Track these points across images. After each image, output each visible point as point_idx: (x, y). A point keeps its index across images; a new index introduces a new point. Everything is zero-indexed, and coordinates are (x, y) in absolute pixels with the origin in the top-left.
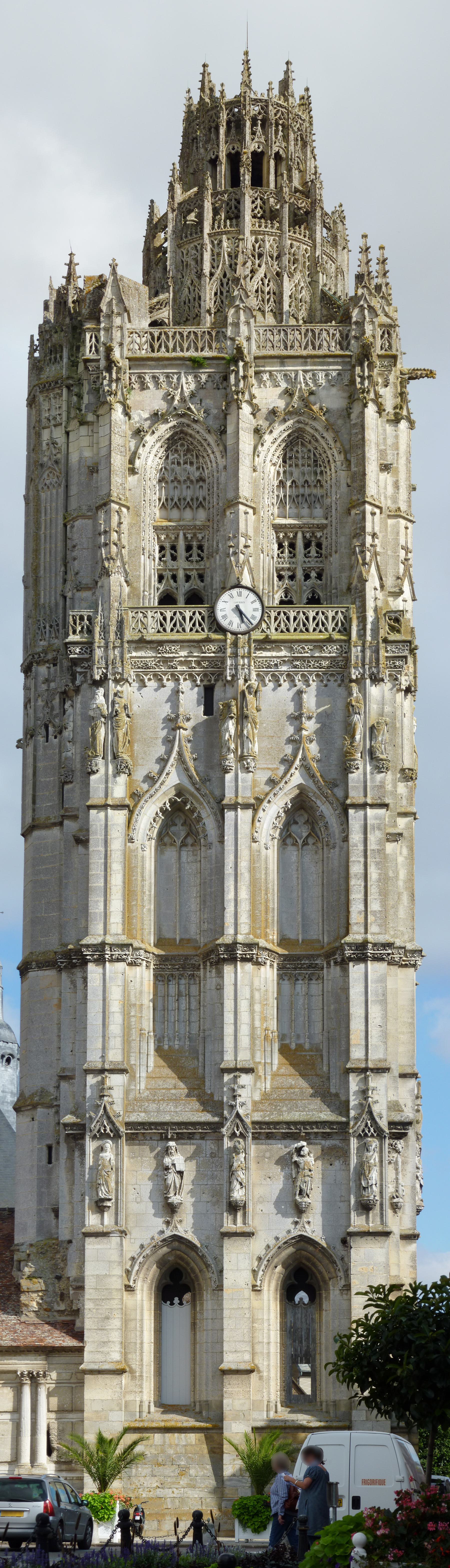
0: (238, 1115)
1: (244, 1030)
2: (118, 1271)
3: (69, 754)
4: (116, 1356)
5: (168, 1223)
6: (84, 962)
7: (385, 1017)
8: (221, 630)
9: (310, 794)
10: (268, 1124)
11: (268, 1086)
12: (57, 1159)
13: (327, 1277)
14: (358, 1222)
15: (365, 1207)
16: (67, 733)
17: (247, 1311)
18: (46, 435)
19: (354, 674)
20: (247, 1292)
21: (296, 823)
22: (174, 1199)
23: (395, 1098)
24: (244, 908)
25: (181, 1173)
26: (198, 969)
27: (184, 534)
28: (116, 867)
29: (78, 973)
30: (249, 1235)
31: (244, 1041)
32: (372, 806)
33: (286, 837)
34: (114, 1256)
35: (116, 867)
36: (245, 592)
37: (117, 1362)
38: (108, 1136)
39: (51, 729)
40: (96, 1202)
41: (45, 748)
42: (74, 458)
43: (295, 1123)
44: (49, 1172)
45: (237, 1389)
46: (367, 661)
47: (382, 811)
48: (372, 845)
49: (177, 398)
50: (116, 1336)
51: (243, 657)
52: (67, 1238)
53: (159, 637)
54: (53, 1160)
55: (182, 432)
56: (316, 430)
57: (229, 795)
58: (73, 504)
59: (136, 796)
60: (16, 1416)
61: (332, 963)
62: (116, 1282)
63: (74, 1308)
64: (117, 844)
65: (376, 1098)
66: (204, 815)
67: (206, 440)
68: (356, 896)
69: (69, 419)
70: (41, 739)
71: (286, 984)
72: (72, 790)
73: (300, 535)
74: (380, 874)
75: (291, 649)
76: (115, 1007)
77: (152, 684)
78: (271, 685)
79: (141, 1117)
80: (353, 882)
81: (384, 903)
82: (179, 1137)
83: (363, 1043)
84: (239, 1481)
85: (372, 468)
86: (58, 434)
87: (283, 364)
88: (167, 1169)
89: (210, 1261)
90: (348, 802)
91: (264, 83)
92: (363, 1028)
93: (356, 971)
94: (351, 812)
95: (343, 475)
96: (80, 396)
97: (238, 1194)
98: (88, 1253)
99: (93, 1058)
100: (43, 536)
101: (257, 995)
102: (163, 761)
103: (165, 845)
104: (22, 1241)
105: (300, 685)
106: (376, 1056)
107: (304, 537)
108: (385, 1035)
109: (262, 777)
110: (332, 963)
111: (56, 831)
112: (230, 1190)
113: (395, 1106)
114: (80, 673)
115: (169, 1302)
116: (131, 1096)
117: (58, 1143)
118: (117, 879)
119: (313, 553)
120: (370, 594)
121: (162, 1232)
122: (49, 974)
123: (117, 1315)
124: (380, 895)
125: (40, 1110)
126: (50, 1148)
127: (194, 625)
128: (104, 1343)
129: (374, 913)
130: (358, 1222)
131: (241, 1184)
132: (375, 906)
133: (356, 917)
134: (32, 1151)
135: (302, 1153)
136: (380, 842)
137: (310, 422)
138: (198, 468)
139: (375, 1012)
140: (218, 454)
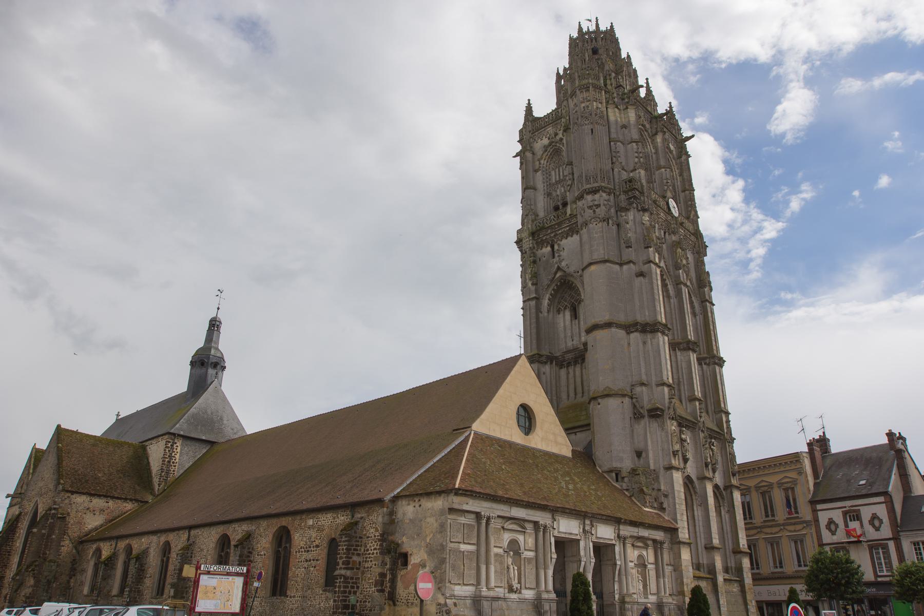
6: (658, 331)
29: (649, 336)
42: (612, 118)
44: (633, 431)
69: (607, 102)
86: (600, 106)
111: (617, 267)
122: (621, 333)
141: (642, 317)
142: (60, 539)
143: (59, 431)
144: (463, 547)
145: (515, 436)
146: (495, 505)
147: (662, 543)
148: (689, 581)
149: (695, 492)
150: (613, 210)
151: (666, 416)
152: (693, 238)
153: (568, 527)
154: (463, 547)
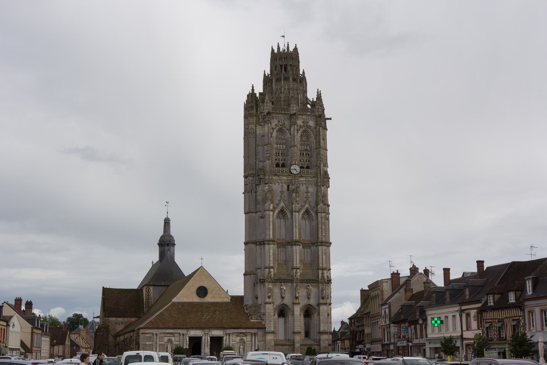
1: (298, 260)
2: (273, 311)
6: (264, 244)
14: (321, 301)
15: (323, 298)
16: (258, 193)
18: (250, 126)
19: (319, 184)
22: (283, 295)
24: (297, 233)
28: (271, 224)
29: (262, 247)
30: (299, 304)
31: (298, 262)
33: (303, 218)
35: (271, 224)
42: (258, 132)
50: (272, 325)
53: (279, 174)
57: (294, 209)
58: (258, 143)
59: (273, 208)
62: (273, 314)
64: (271, 219)
68: (320, 232)
71: (303, 249)
76: (271, 254)
77: (277, 184)
78: (301, 185)
79: (277, 278)
82: (284, 282)
85: (321, 140)
86: (253, 126)
91: (291, 49)
93: (320, 248)
95: (314, 141)
96: (259, 119)
97: (297, 295)
99: (267, 265)
102: (280, 201)
106: (324, 266)
108: (326, 262)
109: (300, 205)
111: (254, 214)
113: (328, 277)
117: (257, 283)
118: (271, 227)
120: (322, 167)
122: (253, 246)
130: (321, 301)
132: (324, 234)
133: (320, 236)
136: (325, 221)
139: (324, 257)
141: (260, 238)
142: (108, 336)
143: (104, 289)
144: (147, 343)
146: (159, 330)
147: (255, 334)
148: (271, 347)
150: (254, 185)
152: (314, 179)
153: (194, 333)
154: (147, 343)
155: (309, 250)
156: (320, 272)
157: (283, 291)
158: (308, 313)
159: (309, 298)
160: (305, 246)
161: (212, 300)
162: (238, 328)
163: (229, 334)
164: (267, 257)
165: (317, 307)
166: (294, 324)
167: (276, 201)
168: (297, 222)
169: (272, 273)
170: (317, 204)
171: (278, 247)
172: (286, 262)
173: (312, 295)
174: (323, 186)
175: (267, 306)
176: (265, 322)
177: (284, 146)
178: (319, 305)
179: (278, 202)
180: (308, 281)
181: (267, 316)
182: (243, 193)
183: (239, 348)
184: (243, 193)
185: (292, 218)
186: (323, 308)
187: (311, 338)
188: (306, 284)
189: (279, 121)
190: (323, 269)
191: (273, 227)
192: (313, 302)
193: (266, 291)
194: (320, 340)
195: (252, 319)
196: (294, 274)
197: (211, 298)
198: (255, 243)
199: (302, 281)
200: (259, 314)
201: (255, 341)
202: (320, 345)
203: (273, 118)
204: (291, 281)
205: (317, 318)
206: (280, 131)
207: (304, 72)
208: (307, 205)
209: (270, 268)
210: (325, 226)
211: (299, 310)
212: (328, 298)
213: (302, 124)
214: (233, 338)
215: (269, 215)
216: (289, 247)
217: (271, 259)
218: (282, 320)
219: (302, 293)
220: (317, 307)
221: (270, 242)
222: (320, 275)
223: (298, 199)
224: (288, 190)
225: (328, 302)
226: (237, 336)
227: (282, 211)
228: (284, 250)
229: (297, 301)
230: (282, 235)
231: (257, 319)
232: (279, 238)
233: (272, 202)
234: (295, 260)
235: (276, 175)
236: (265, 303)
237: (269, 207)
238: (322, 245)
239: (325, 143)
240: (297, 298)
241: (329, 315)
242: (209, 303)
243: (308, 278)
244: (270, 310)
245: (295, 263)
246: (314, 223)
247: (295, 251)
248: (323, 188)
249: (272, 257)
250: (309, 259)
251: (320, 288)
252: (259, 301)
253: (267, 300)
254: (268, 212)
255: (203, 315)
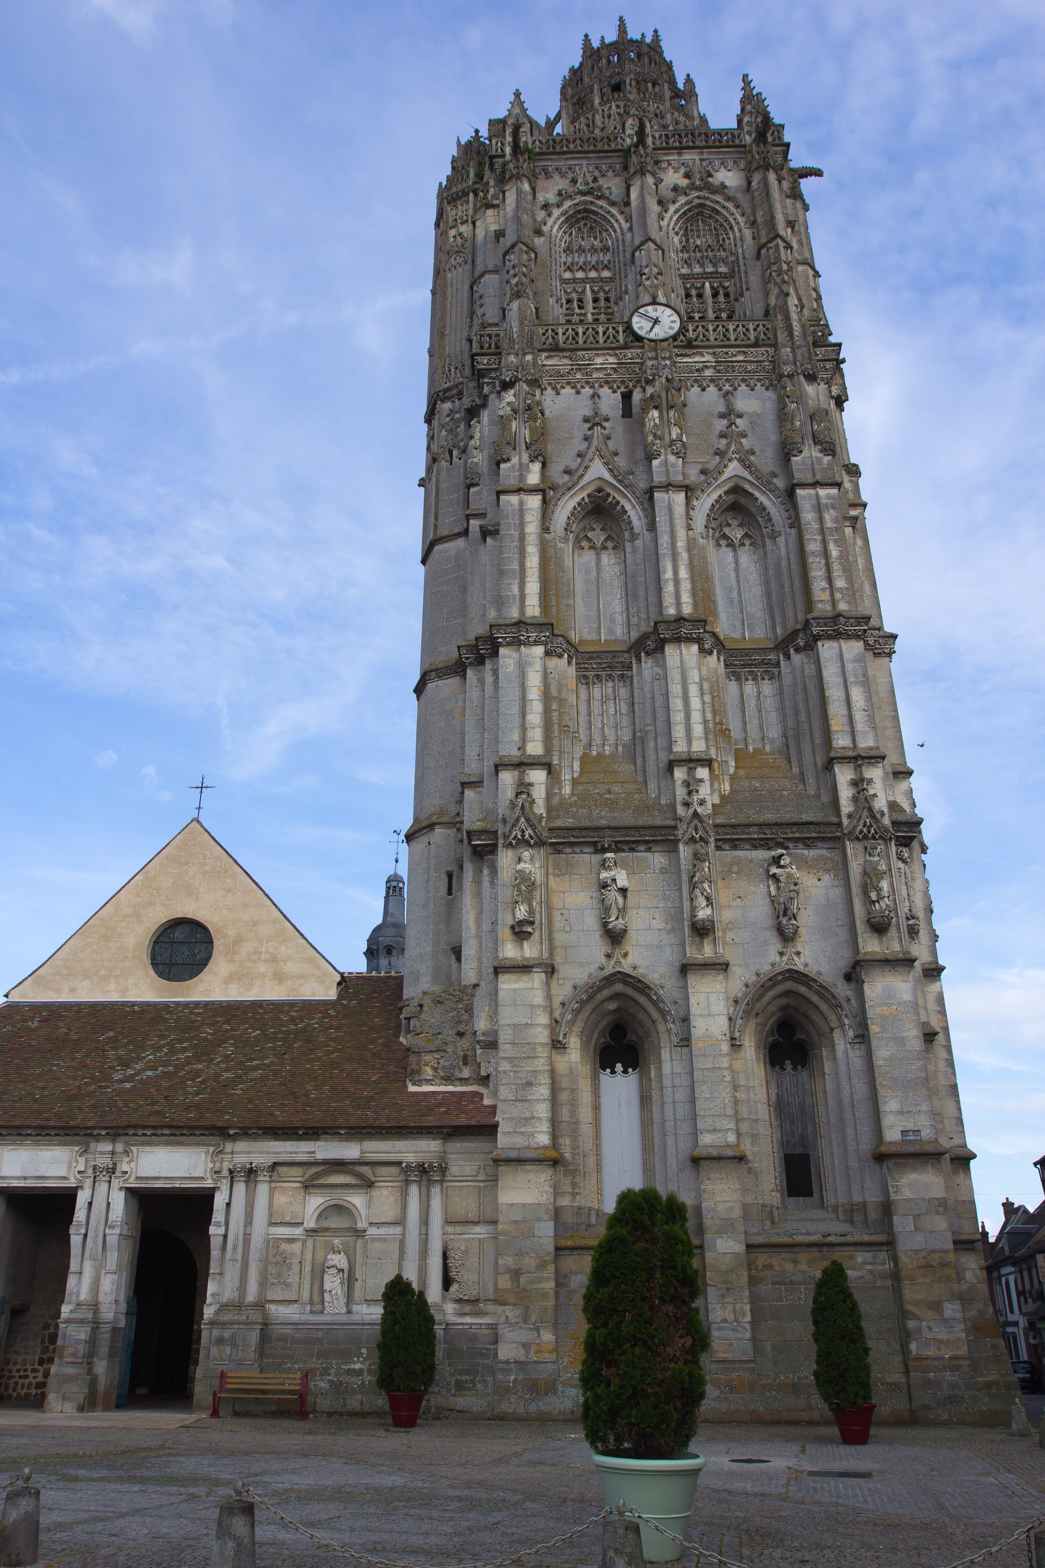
0: (696, 814)
1: (696, 717)
2: (543, 1019)
3: (475, 460)
4: (543, 1139)
5: (608, 956)
7: (869, 699)
8: (639, 339)
9: (747, 487)
10: (733, 826)
11: (727, 788)
12: (460, 888)
13: (826, 1030)
14: (871, 945)
15: (879, 928)
17: (726, 1073)
19: (787, 369)
20: (725, 1047)
21: (729, 525)
22: (616, 923)
23: (890, 798)
24: (686, 586)
25: (623, 891)
26: (630, 668)
27: (591, 288)
31: (698, 730)
32: (823, 485)
34: (539, 998)
36: (660, 308)
37: (545, 1148)
38: (527, 844)
39: (455, 453)
40: (512, 927)
41: (448, 470)
43: (769, 825)
45: (719, 1187)
46: (799, 357)
47: (834, 491)
48: (829, 524)
49: (580, 181)
50: (543, 1110)
51: (664, 359)
52: (473, 980)
54: (454, 892)
55: (586, 210)
56: (717, 202)
57: (658, 478)
60: (398, 1230)
61: (792, 651)
62: (542, 1036)
63: (483, 1073)
65: (872, 792)
66: (628, 507)
67: (609, 212)
68: (817, 573)
70: (444, 464)
71: (733, 686)
72: (480, 492)
73: (707, 285)
74: (840, 551)
75: (714, 354)
76: (534, 694)
80: (810, 560)
81: (850, 579)
83: (847, 729)
84: (733, 1330)
87: (680, 154)
88: (604, 886)
89: (669, 1006)
90: (795, 481)
92: (845, 712)
93: (827, 649)
94: (799, 492)
95: (747, 233)
97: (704, 913)
98: (501, 993)
100: (449, 305)
101: (706, 685)
103: (583, 548)
104: (412, 994)
105: (727, 387)
106: (866, 742)
107: (712, 287)
108: (872, 720)
110: (792, 651)
111: (460, 542)
112: (693, 909)
113: (893, 806)
114: (488, 384)
115: (608, 1071)
116: (555, 801)
117: (461, 868)
119: (721, 298)
121: (602, 969)
122: (450, 684)
123: (545, 1079)
124: (844, 572)
125: (438, 831)
126: (450, 876)
127: (608, 338)
128: (526, 1119)
129: (841, 590)
130: (871, 945)
131: (707, 899)
132: (840, 583)
134: (427, 881)
135: (782, 863)
136: (836, 520)
137: (711, 196)
138: (602, 241)
139: (857, 695)
140: (622, 221)
145: (144, 988)
148: (530, 1262)
149: (663, 1013)
151: (501, 841)
152: (761, 353)
155: (768, 688)
156: (844, 775)
157: (613, 896)
158: (791, 1030)
159: (786, 936)
160: (742, 662)
161: (234, 994)
162: (313, 1133)
163: (251, 1173)
164: (510, 708)
165: (843, 990)
166: (693, 1100)
167: (564, 458)
168: (681, 533)
169: (539, 793)
170: (786, 451)
171: (584, 679)
172: (635, 748)
173: (807, 919)
174: (811, 378)
175: (508, 984)
176: (495, 1094)
177: (606, 274)
178: (853, 975)
179: (573, 464)
180: (776, 836)
181: (505, 1049)
182: (422, 483)
183: (319, 1272)
184: (422, 483)
185: (652, 526)
186: (886, 991)
187: (830, 1200)
188: (763, 855)
189: (574, 181)
190: (859, 759)
191: (533, 552)
192: (816, 955)
193: (506, 894)
194: (887, 1208)
195: (415, 1076)
196: (681, 792)
197: (230, 979)
198: (458, 669)
199: (732, 836)
200: (465, 1043)
201: (425, 1221)
202: (890, 1244)
203: (548, 176)
204: (660, 837)
205: (856, 1056)
206: (584, 219)
207: (689, 80)
208: (734, 468)
209: (522, 765)
210: (841, 542)
211: (720, 1007)
212: (913, 932)
213: (684, 182)
214: (281, 1199)
215: (522, 510)
216: (648, 665)
217: (535, 717)
218: (620, 1087)
219: (739, 903)
220: (843, 990)
221: (520, 632)
222: (845, 793)
223: (675, 432)
224: (627, 411)
225: (919, 951)
226: (308, 1186)
227: (600, 510)
228: (623, 692)
229: (708, 951)
230: (600, 611)
231: (448, 1079)
232: (593, 637)
233: (541, 456)
234: (678, 717)
235: (555, 349)
236: (497, 971)
237: (522, 478)
238: (837, 636)
239: (805, 242)
240: (702, 931)
241: (934, 1036)
242: (207, 1004)
243: (769, 817)
244: (523, 1007)
245: (678, 732)
246: (783, 546)
247: (674, 675)
248: (810, 390)
249: (536, 708)
250: (774, 732)
251: (855, 868)
252: (469, 972)
253: (510, 951)
254: (514, 499)
255: (126, 1064)
